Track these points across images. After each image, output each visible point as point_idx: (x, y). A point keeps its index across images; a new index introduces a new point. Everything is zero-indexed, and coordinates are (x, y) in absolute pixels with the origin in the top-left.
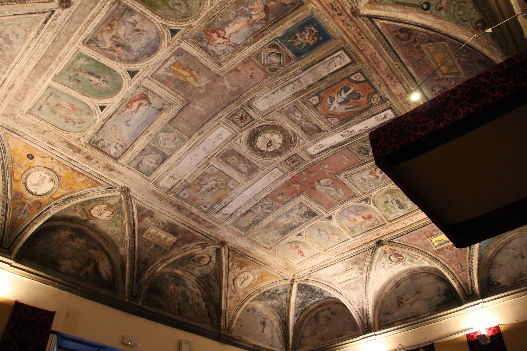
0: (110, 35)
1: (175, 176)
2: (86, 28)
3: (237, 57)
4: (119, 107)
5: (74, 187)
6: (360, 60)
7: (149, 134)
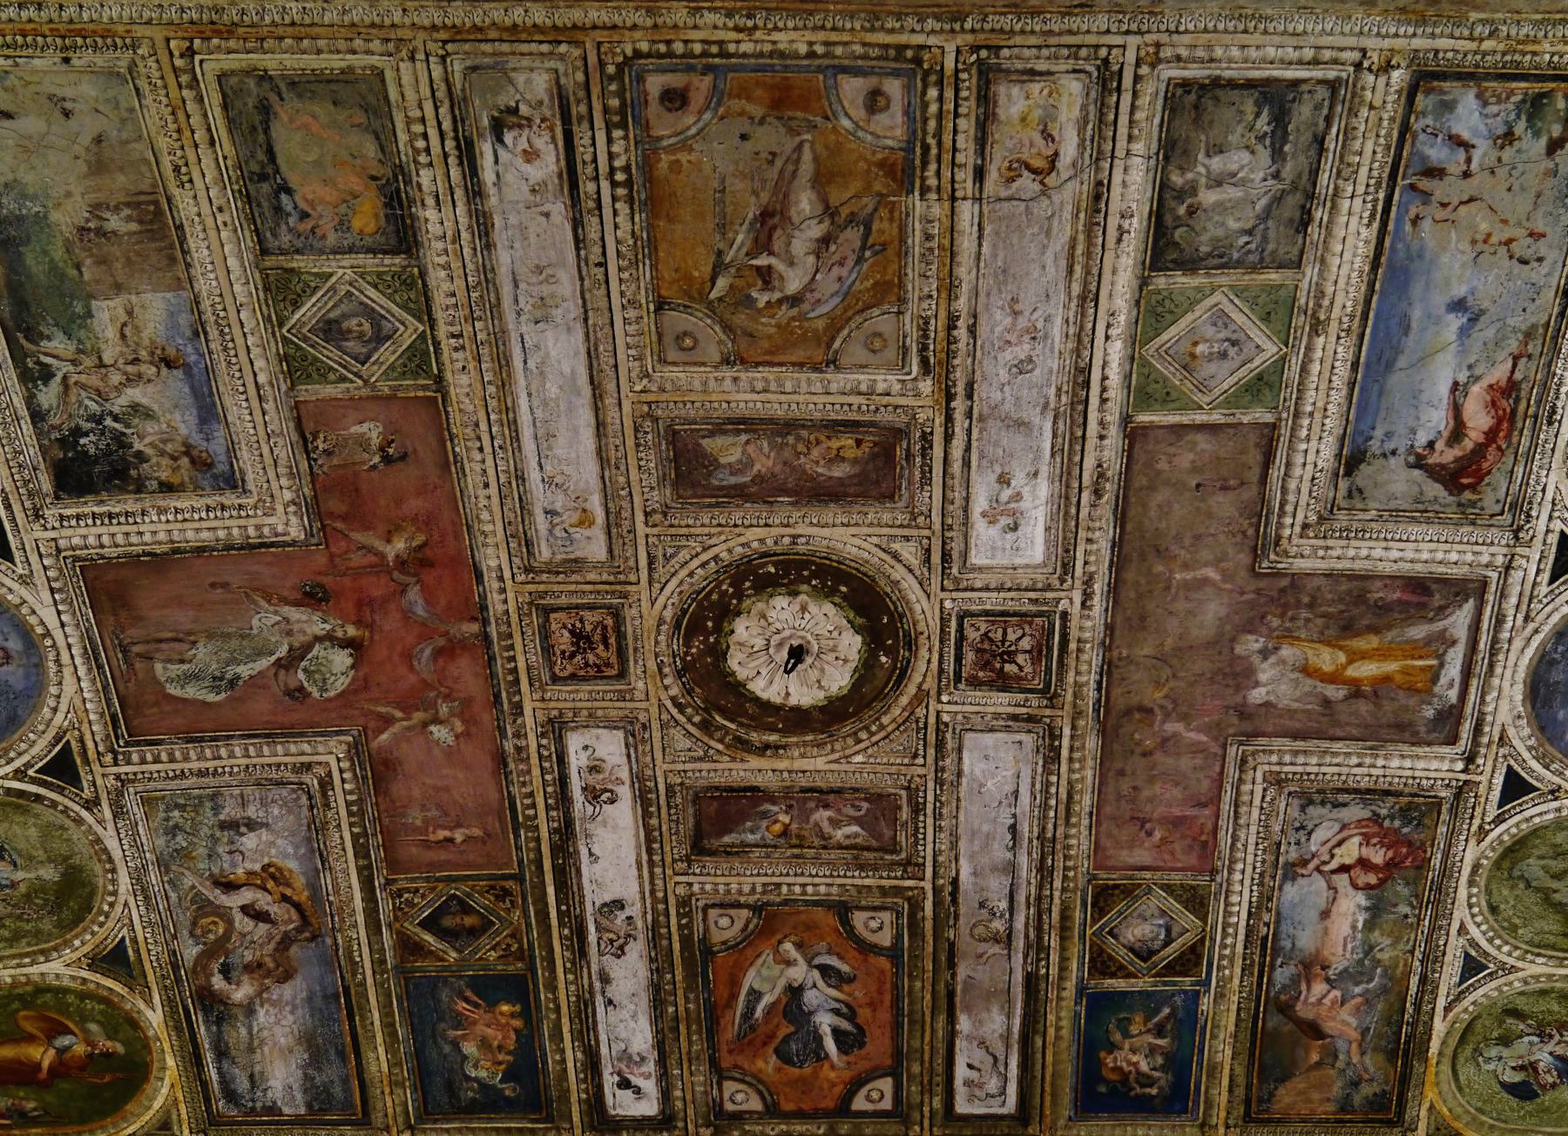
1: (1027, 184)
3: (1251, 848)
7: (1333, 328)
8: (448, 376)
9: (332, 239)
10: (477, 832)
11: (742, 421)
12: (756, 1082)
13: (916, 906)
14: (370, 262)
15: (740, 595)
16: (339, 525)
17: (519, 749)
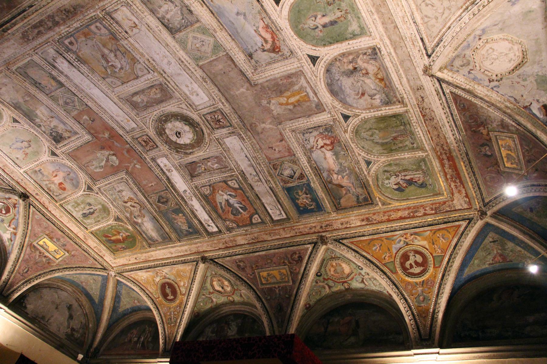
1: (134, 29)
2: (392, 63)
4: (270, 18)
7: (217, 30)
12: (232, 221)
15: (163, 125)
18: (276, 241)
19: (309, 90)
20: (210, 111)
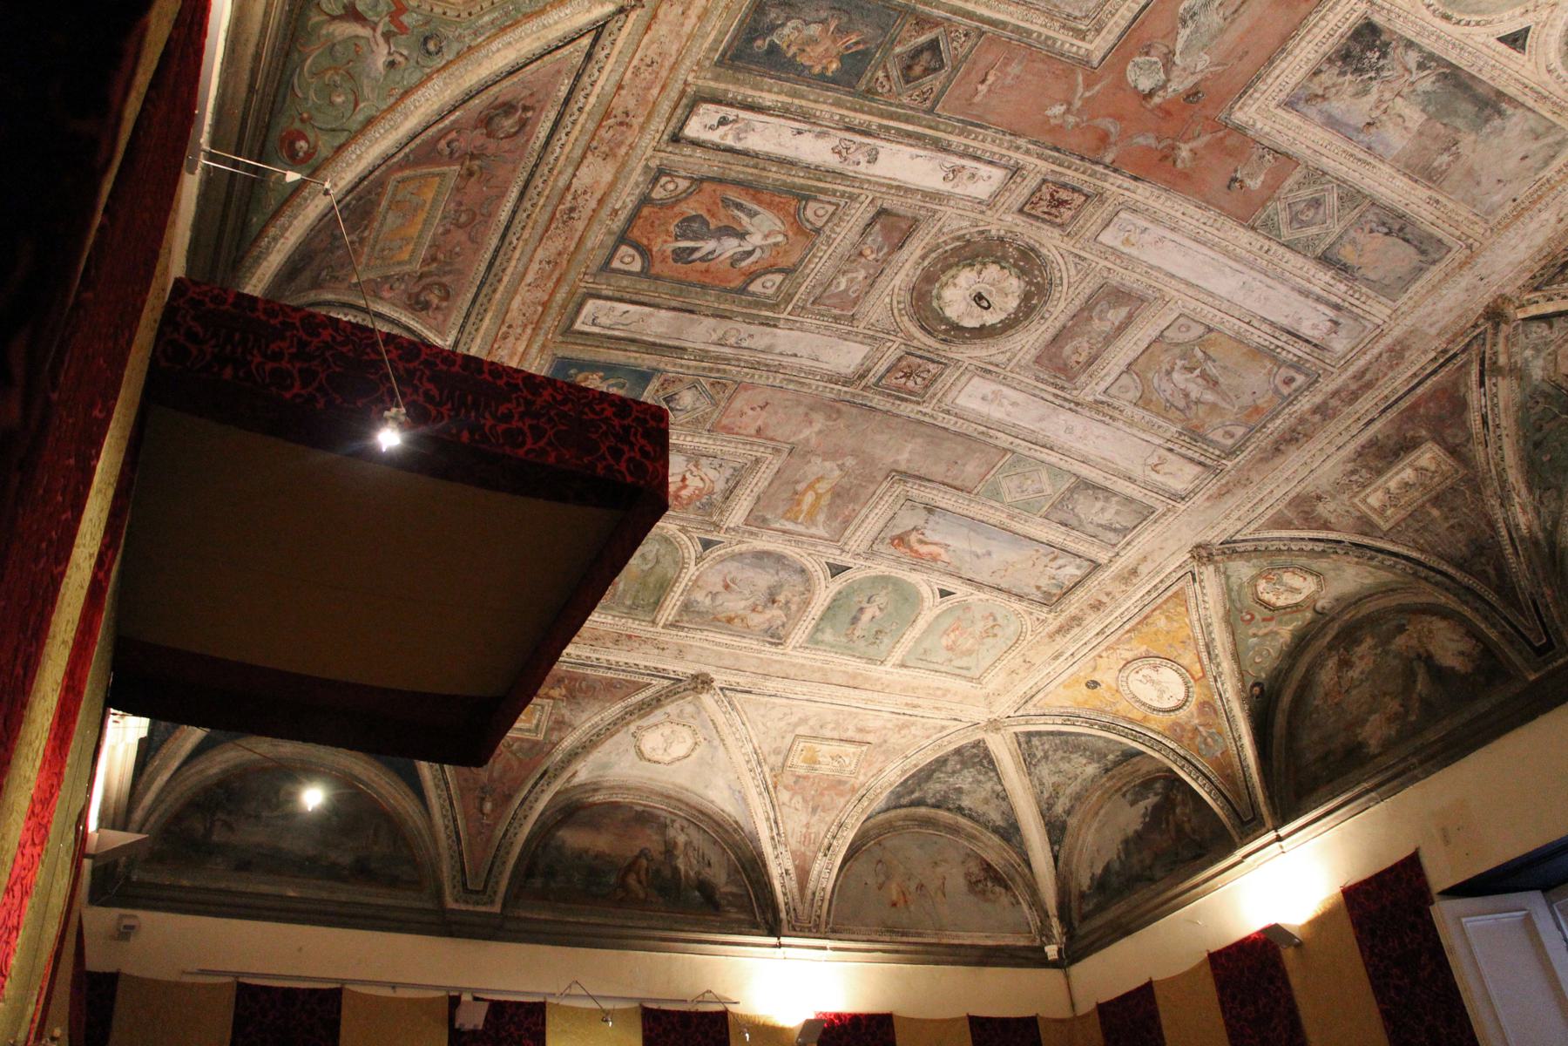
0: (753, 615)
5: (1182, 634)
6: (571, 294)
8: (1251, 233)
9: (1352, 233)
10: (977, 99)
11: (1127, 325)
13: (773, 307)
14: (1328, 241)
15: (1029, 283)
16: (1221, 134)
17: (1018, 148)
18: (520, 268)
19: (801, 529)
20: (938, 385)
